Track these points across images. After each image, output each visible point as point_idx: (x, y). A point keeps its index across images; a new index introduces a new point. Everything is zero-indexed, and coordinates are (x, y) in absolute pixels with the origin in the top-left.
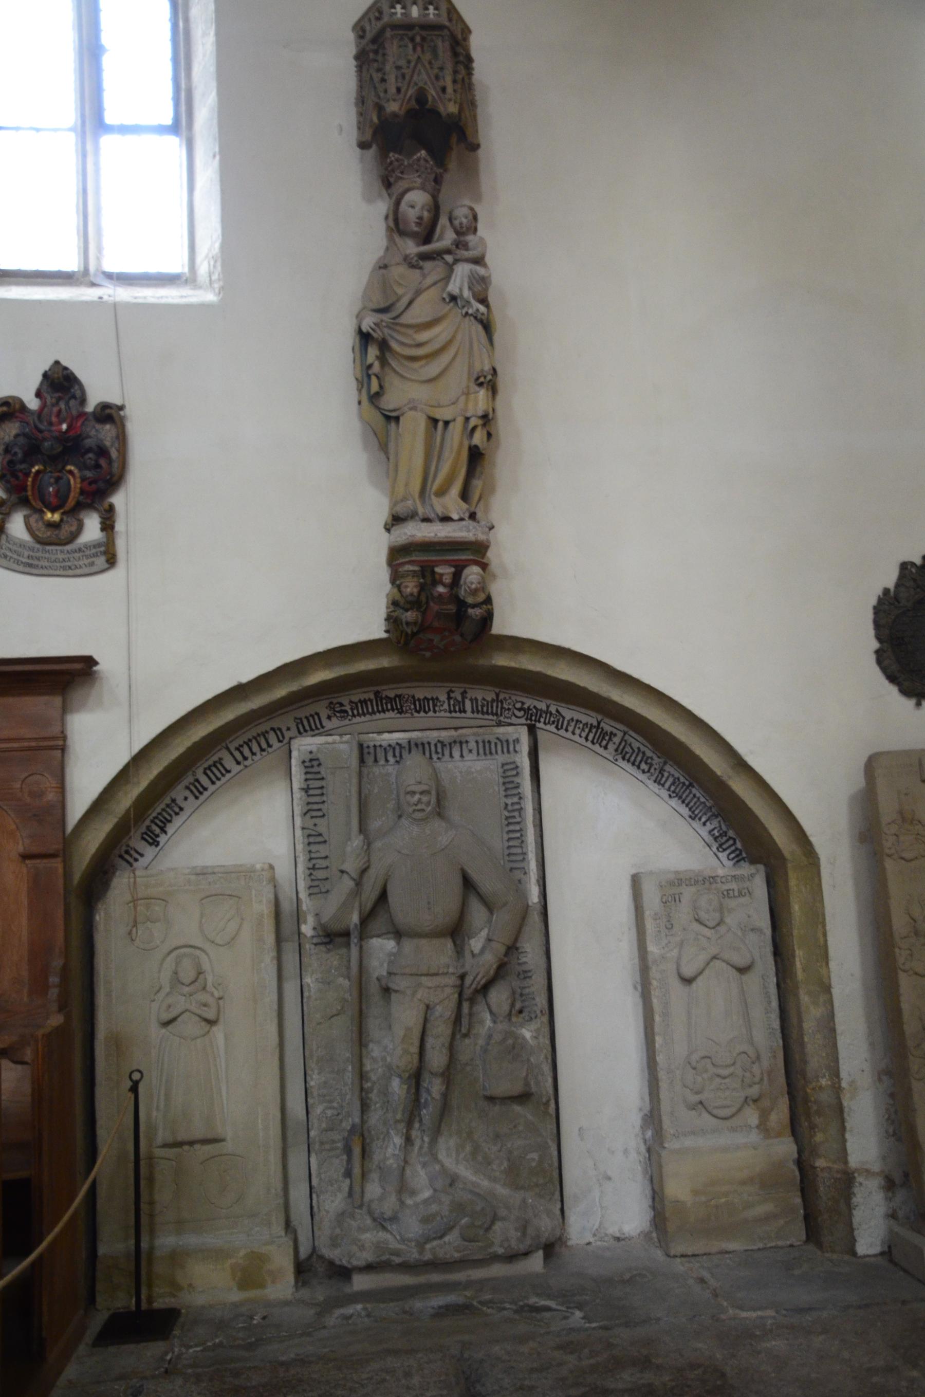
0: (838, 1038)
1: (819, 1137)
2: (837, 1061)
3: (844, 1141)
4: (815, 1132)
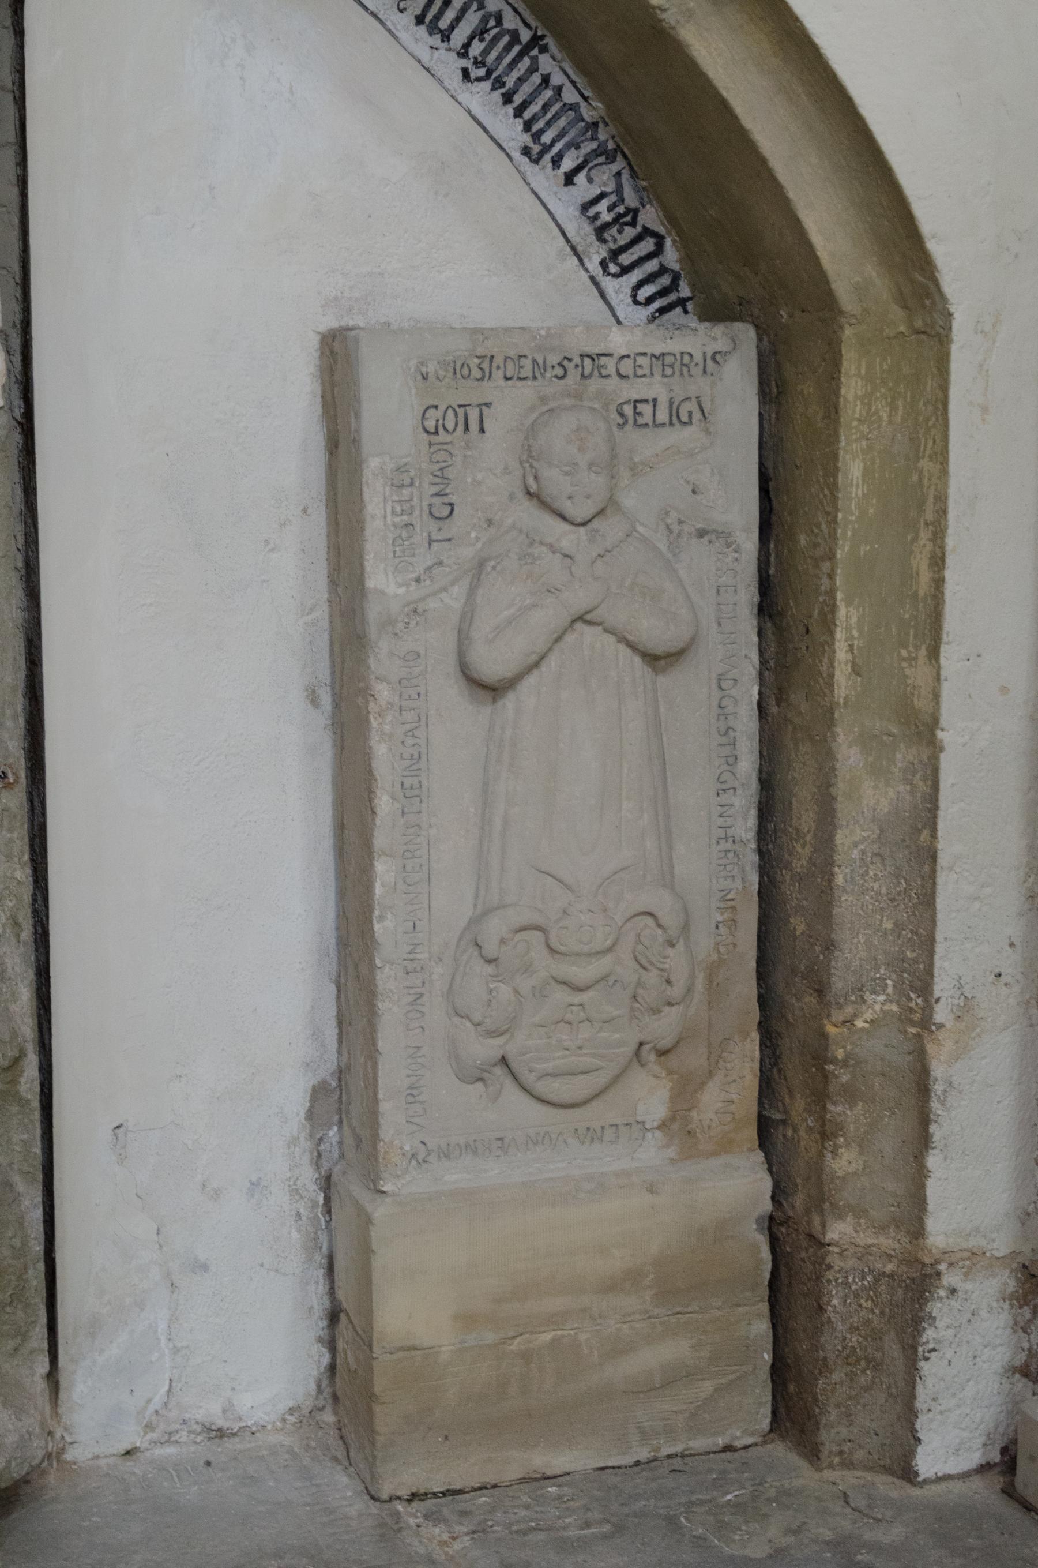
0: (941, 878)
1: (844, 1162)
2: (928, 944)
3: (920, 1175)
4: (836, 1147)
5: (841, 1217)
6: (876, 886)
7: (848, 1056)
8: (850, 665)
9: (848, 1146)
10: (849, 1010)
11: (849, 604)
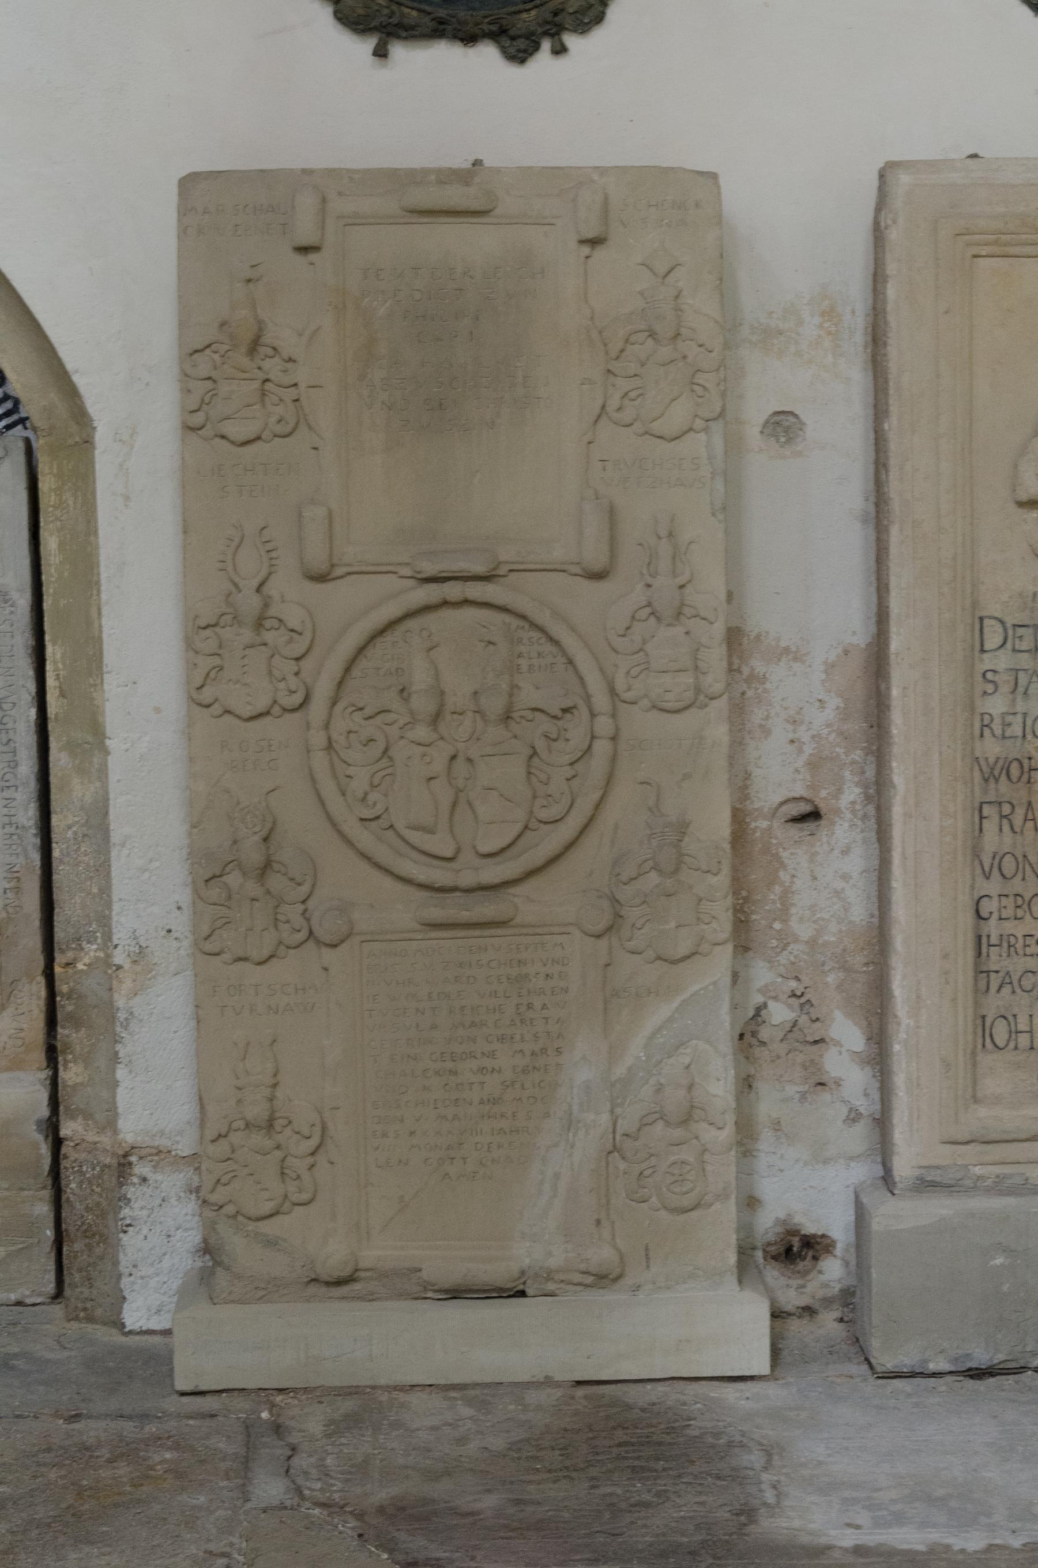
5: (73, 1118)
6: (86, 859)
7: (72, 991)
8: (58, 690)
9: (75, 1061)
10: (70, 955)
11: (54, 644)
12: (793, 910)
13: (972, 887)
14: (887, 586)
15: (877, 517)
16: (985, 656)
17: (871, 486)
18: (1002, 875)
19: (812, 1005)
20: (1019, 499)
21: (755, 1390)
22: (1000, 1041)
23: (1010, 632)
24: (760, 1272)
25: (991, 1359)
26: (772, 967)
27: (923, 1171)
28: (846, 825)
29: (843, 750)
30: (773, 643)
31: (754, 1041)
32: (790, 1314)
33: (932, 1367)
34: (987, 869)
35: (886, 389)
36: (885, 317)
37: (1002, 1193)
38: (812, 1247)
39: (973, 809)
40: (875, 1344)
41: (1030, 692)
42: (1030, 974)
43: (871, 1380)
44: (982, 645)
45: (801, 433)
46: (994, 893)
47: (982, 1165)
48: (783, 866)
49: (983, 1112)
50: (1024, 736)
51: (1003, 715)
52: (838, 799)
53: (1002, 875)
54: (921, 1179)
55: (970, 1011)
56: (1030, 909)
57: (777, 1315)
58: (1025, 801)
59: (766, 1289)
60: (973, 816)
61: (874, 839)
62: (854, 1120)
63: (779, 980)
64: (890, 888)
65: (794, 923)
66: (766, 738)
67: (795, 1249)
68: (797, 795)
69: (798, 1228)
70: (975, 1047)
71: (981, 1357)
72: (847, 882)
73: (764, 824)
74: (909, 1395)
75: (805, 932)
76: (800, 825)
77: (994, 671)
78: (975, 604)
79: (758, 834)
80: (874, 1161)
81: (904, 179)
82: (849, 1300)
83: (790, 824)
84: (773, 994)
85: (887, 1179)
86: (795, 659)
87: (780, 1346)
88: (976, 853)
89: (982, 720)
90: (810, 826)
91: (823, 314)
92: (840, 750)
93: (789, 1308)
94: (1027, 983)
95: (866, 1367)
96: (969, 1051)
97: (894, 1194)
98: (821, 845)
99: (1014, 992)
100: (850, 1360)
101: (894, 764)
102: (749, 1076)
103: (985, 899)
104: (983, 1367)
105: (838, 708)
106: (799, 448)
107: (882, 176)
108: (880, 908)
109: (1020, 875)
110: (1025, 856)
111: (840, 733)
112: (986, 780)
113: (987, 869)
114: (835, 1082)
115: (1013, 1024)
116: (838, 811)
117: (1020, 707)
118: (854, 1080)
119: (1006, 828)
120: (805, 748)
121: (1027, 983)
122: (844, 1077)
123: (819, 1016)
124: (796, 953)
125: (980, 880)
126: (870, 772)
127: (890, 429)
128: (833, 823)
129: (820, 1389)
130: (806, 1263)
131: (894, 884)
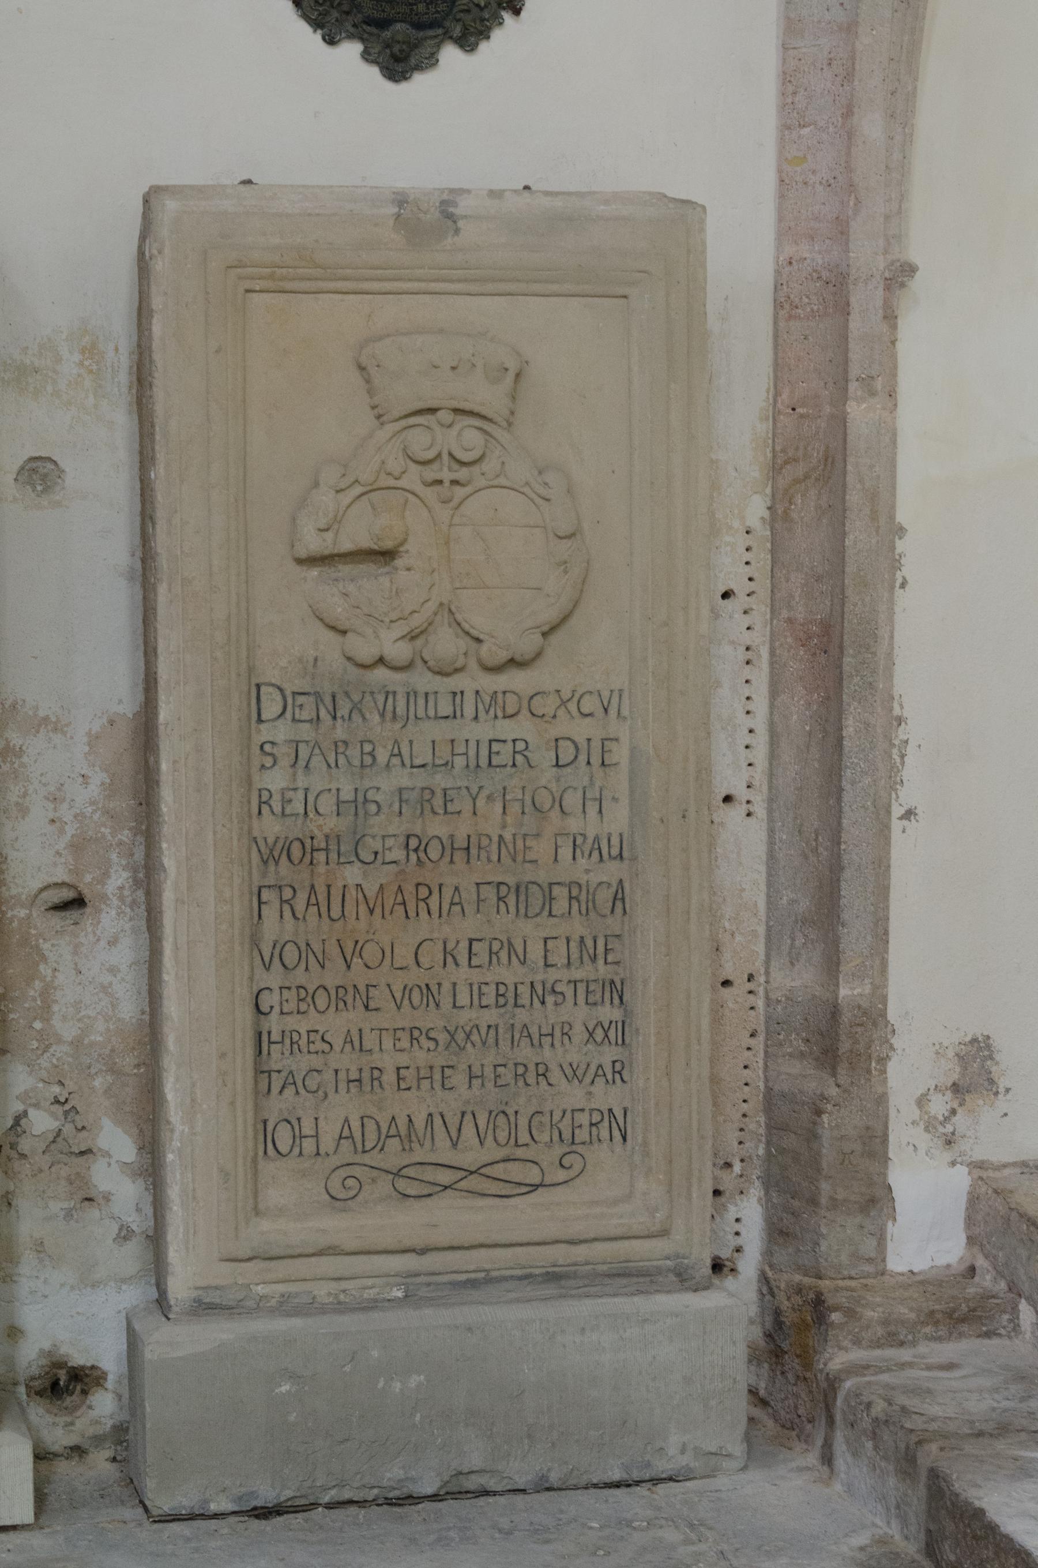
12: (55, 1008)
13: (251, 979)
14: (155, 650)
15: (144, 575)
16: (262, 727)
17: (137, 540)
18: (284, 965)
19: (78, 1112)
20: (297, 556)
21: (18, 1541)
22: (284, 1148)
23: (290, 700)
24: (23, 1411)
25: (278, 1495)
26: (32, 1071)
27: (200, 1292)
28: (114, 913)
29: (108, 830)
30: (31, 713)
31: (13, 1154)
32: (56, 1455)
33: (213, 1507)
34: (267, 959)
35: (153, 434)
36: (150, 356)
37: (288, 1315)
38: (81, 1380)
39: (251, 893)
40: (150, 1485)
41: (311, 766)
42: (315, 1073)
43: (147, 1524)
44: (259, 715)
45: (60, 481)
46: (275, 986)
47: (263, 1283)
48: (44, 958)
49: (265, 1225)
50: (306, 813)
51: (283, 791)
52: (104, 884)
53: (284, 965)
54: (198, 1301)
55: (250, 1115)
56: (314, 1003)
57: (41, 1456)
58: (307, 884)
59: (29, 1429)
60: (251, 900)
61: (144, 928)
62: (125, 1239)
63: (41, 1085)
64: (160, 981)
65: (56, 1022)
66: (23, 818)
67: (62, 1383)
68: (60, 881)
69: (65, 1359)
70: (256, 1154)
71: (267, 1494)
72: (115, 976)
73: (23, 913)
74: (188, 1540)
75: (68, 1031)
76: (63, 914)
77: (272, 743)
78: (251, 670)
79: (15, 924)
80: (148, 1283)
81: (171, 205)
82: (122, 1437)
83: (52, 912)
84: (34, 1101)
85: (162, 1303)
86: (56, 729)
87: (45, 1491)
88: (255, 942)
89: (260, 796)
90: (73, 914)
91: (83, 352)
92: (106, 831)
93: (56, 1448)
94: (311, 1084)
95: (141, 1510)
96: (249, 1159)
97: (169, 1319)
98: (86, 936)
99: (297, 1093)
100: (123, 1502)
101: (164, 845)
102: (8, 1193)
103: (266, 992)
104: (270, 1505)
105: (103, 784)
106: (58, 498)
107: (146, 201)
108: (152, 1003)
109: (303, 965)
110: (308, 945)
111: (106, 812)
112: (265, 862)
113: (267, 959)
114: (103, 1197)
115: (297, 1128)
116: (104, 898)
117: (301, 782)
118: (125, 1193)
119: (287, 913)
120: (67, 828)
121: (312, 1083)
122: (113, 1192)
123: (86, 1124)
124: (58, 1055)
125: (259, 970)
126: (139, 854)
127: (156, 478)
128: (99, 911)
129: (90, 1537)
130: (74, 1397)
131: (166, 977)
